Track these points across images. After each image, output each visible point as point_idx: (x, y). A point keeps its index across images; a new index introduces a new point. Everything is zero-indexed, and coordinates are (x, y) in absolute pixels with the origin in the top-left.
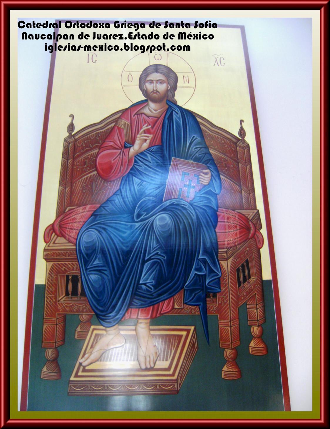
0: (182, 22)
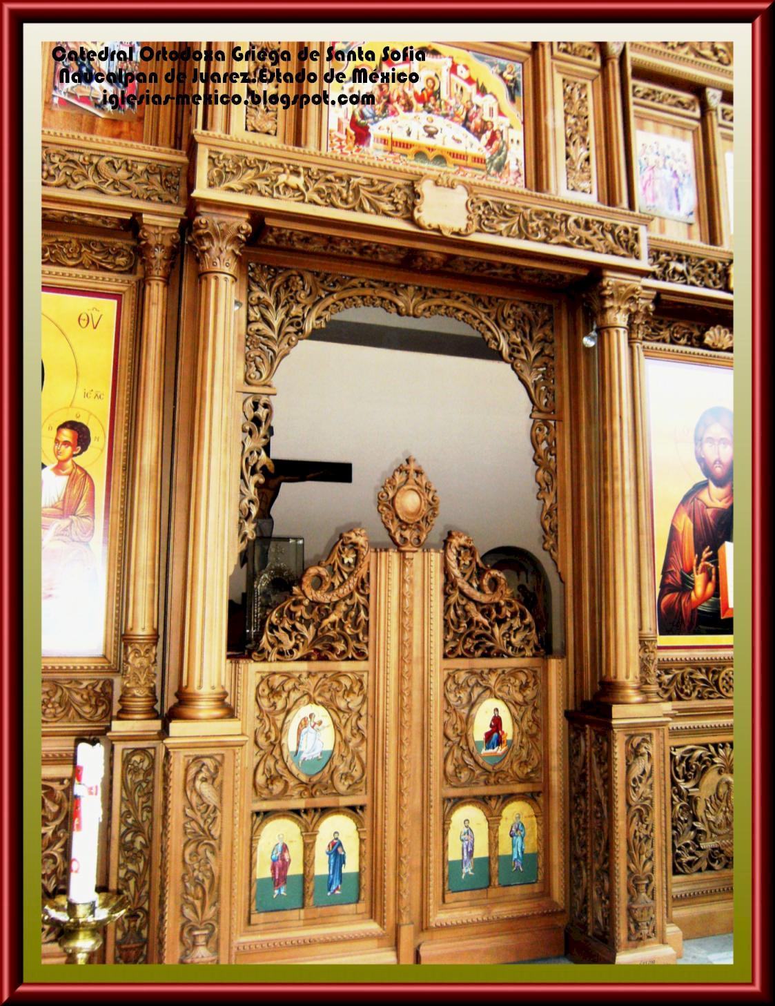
0: (360, 49)
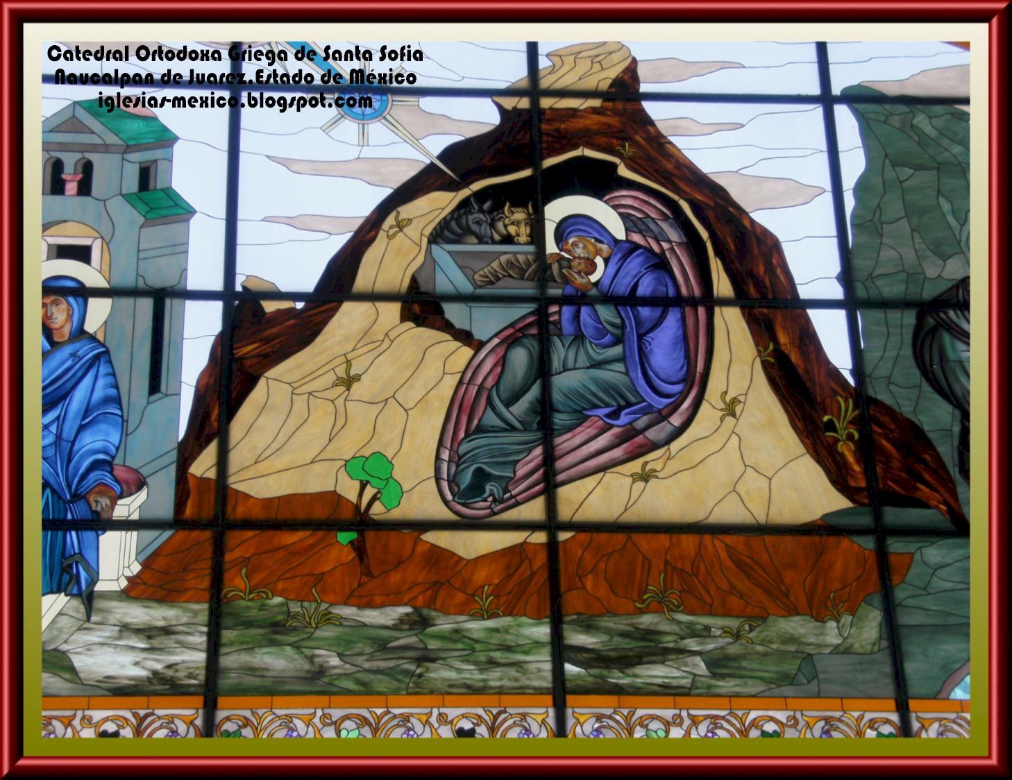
0: (357, 47)
